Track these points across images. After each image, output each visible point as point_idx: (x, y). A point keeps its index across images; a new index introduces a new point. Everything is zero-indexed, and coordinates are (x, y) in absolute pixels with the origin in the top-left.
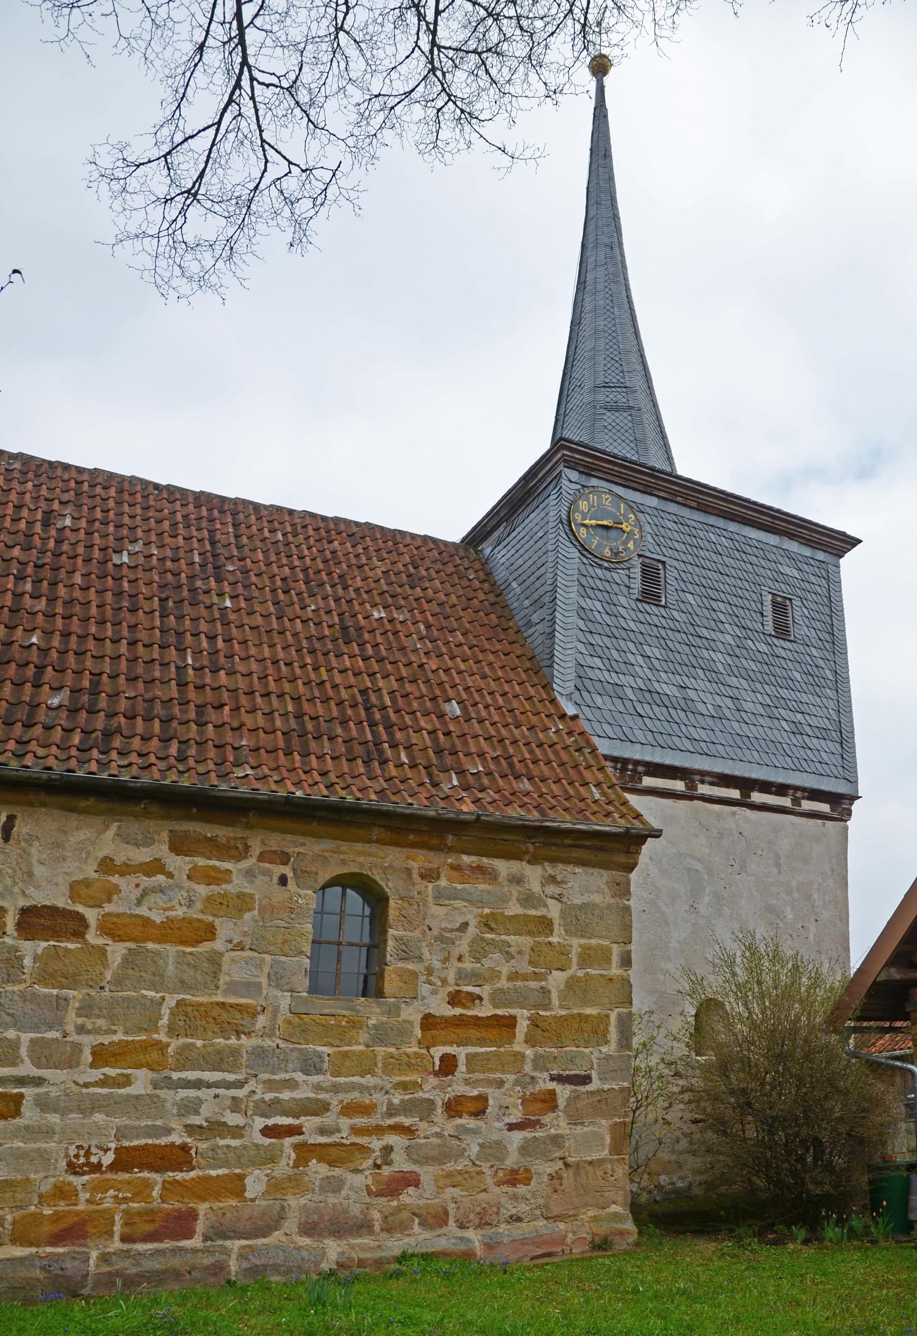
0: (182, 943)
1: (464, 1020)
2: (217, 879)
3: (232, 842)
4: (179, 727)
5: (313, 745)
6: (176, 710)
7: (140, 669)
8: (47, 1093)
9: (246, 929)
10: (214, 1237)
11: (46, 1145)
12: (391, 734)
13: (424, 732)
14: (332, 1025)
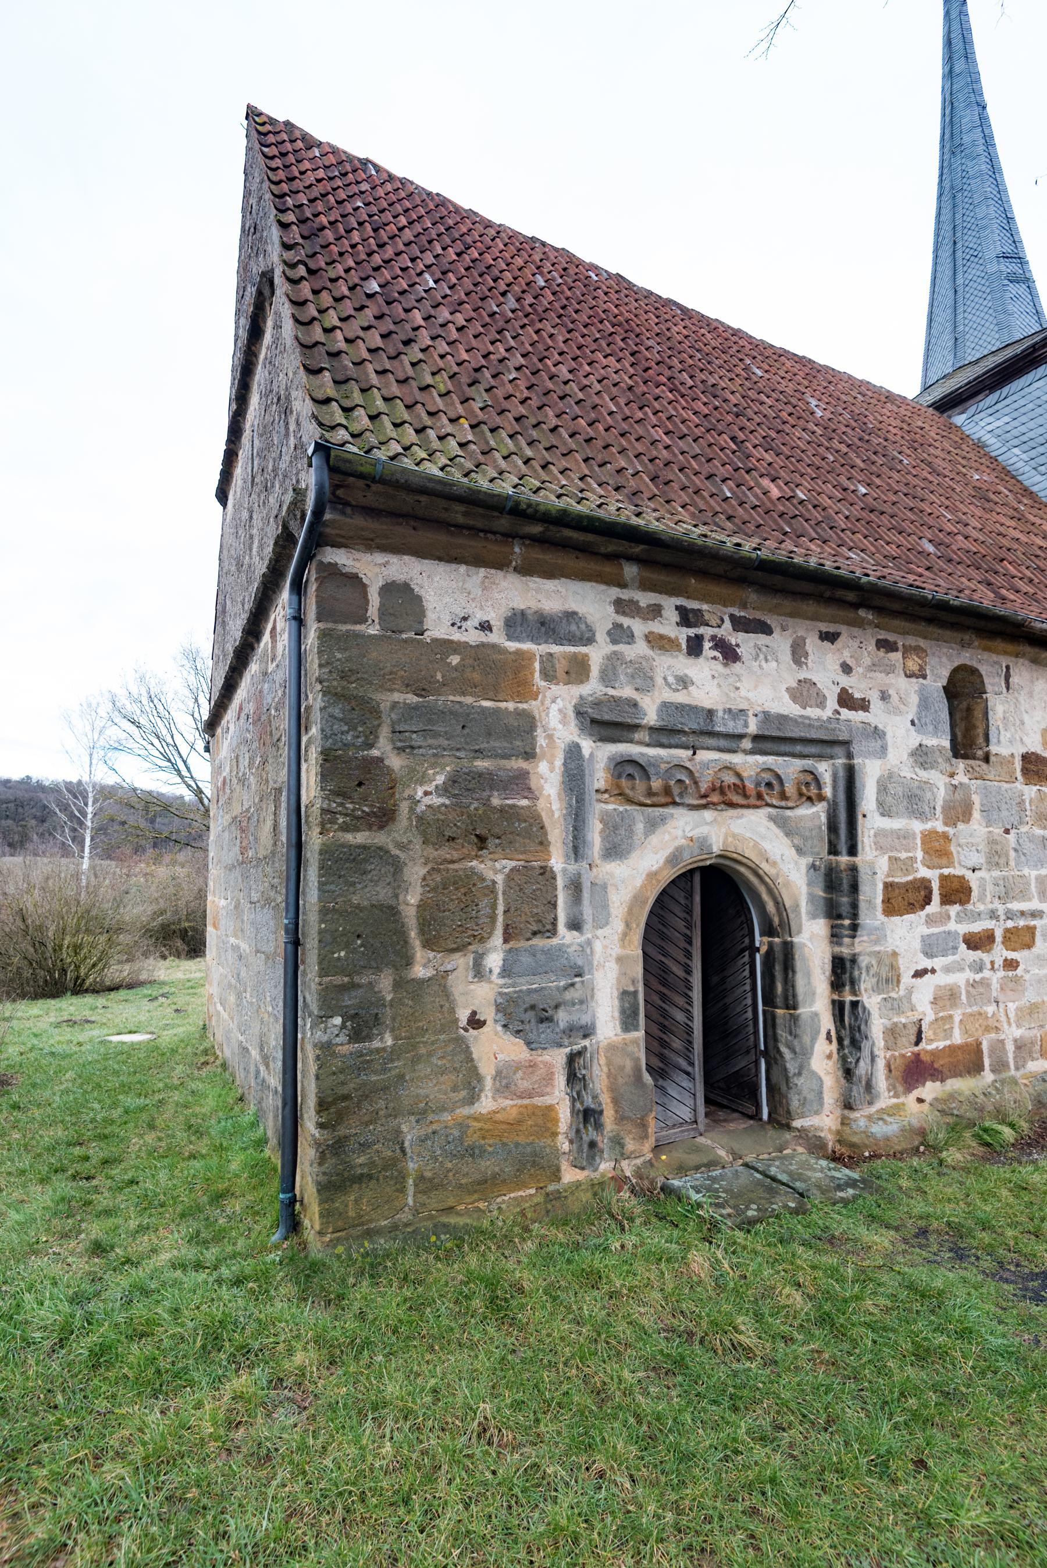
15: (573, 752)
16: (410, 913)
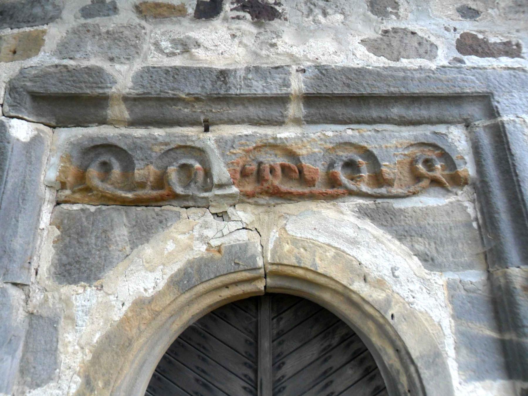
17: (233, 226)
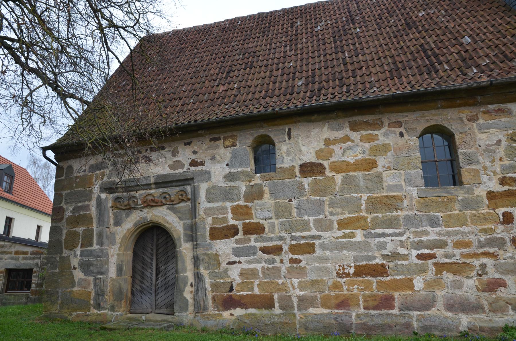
0: (364, 170)
1: (511, 193)
2: (373, 139)
3: (375, 121)
4: (346, 80)
5: (403, 73)
6: (344, 74)
7: (329, 63)
8: (323, 242)
9: (390, 160)
10: (404, 309)
11: (327, 265)
12: (438, 59)
13: (454, 54)
14: (440, 201)
15: (99, 198)
16: (63, 241)
17: (142, 213)
